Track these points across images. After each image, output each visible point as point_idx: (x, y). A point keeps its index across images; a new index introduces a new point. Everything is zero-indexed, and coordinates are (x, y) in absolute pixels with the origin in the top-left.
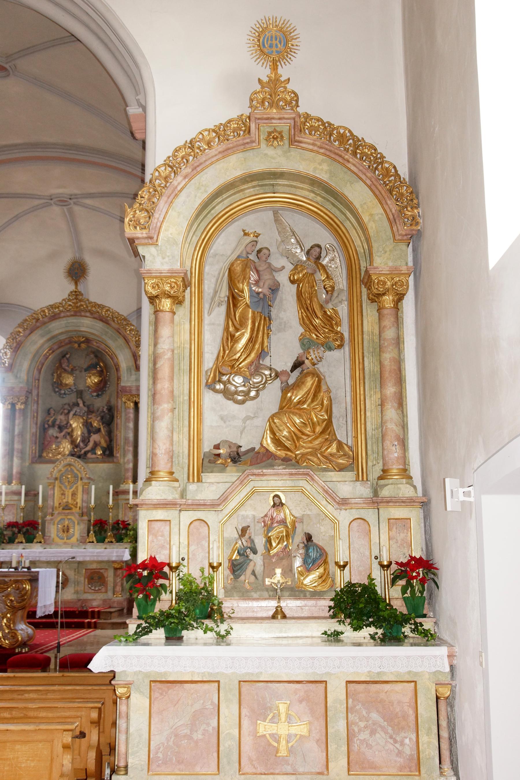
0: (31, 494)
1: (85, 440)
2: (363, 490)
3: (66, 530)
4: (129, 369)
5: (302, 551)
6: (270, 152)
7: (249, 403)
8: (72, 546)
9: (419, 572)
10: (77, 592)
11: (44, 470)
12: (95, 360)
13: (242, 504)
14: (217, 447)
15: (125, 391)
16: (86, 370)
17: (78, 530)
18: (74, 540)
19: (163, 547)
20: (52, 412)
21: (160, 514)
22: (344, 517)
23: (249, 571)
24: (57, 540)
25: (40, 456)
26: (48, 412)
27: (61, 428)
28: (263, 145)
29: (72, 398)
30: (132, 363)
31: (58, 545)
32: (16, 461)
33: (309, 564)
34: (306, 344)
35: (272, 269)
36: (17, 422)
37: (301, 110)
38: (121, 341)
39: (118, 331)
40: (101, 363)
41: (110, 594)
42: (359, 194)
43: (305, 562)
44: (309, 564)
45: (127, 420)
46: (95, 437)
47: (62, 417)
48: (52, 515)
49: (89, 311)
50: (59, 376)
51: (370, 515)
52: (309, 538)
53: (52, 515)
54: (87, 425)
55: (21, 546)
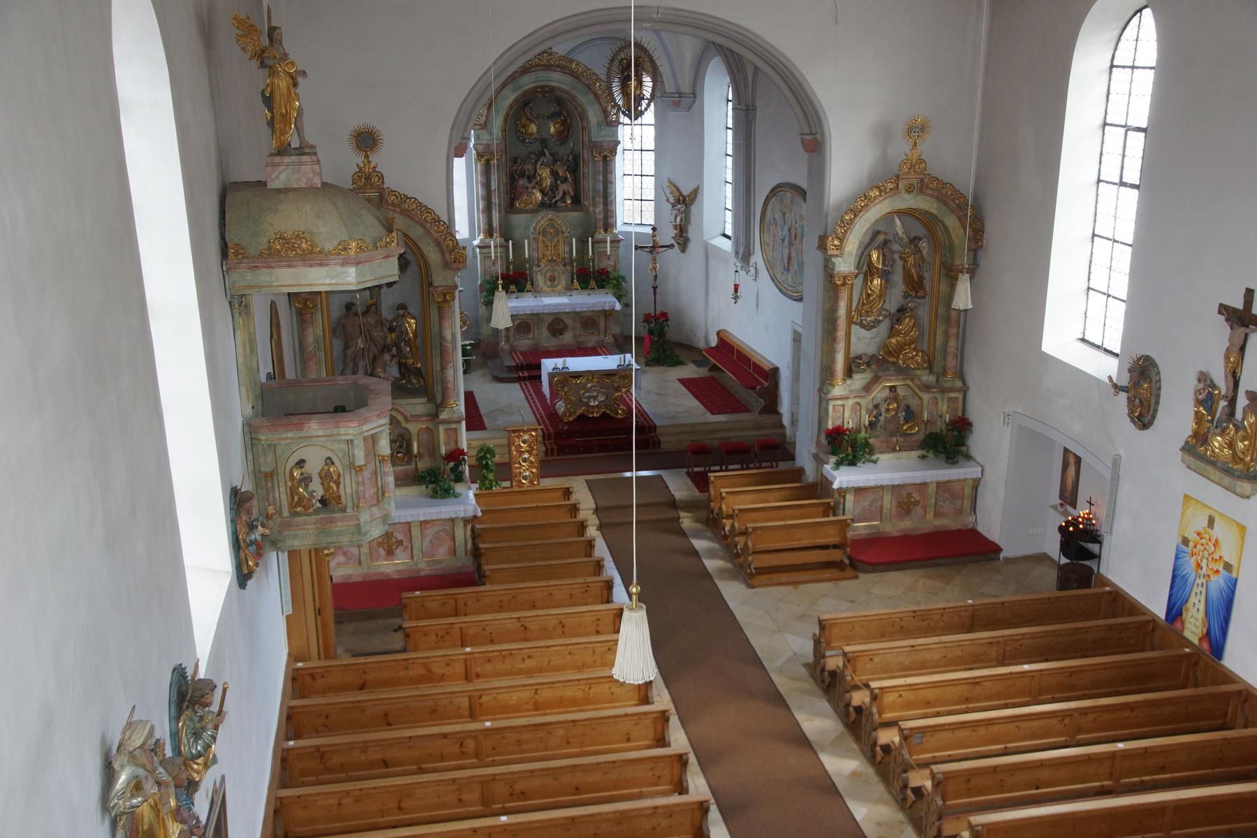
0: (518, 247)
1: (554, 188)
2: (932, 379)
3: (553, 279)
4: (599, 125)
6: (906, 196)
8: (560, 294)
9: (962, 426)
10: (574, 336)
11: (519, 220)
12: (557, 109)
14: (859, 357)
15: (595, 146)
16: (548, 118)
17: (563, 280)
18: (559, 288)
20: (519, 161)
21: (840, 402)
22: (926, 397)
24: (545, 288)
25: (512, 204)
26: (515, 160)
27: (530, 179)
29: (538, 147)
30: (601, 118)
31: (547, 294)
32: (496, 215)
33: (907, 420)
35: (893, 253)
36: (494, 177)
38: (591, 97)
39: (588, 86)
40: (563, 110)
41: (602, 336)
42: (951, 222)
44: (907, 420)
45: (596, 174)
46: (563, 187)
47: (529, 167)
48: (538, 266)
49: (558, 66)
50: (524, 126)
51: (939, 396)
52: (908, 407)
53: (538, 266)
54: (554, 174)
55: (514, 295)
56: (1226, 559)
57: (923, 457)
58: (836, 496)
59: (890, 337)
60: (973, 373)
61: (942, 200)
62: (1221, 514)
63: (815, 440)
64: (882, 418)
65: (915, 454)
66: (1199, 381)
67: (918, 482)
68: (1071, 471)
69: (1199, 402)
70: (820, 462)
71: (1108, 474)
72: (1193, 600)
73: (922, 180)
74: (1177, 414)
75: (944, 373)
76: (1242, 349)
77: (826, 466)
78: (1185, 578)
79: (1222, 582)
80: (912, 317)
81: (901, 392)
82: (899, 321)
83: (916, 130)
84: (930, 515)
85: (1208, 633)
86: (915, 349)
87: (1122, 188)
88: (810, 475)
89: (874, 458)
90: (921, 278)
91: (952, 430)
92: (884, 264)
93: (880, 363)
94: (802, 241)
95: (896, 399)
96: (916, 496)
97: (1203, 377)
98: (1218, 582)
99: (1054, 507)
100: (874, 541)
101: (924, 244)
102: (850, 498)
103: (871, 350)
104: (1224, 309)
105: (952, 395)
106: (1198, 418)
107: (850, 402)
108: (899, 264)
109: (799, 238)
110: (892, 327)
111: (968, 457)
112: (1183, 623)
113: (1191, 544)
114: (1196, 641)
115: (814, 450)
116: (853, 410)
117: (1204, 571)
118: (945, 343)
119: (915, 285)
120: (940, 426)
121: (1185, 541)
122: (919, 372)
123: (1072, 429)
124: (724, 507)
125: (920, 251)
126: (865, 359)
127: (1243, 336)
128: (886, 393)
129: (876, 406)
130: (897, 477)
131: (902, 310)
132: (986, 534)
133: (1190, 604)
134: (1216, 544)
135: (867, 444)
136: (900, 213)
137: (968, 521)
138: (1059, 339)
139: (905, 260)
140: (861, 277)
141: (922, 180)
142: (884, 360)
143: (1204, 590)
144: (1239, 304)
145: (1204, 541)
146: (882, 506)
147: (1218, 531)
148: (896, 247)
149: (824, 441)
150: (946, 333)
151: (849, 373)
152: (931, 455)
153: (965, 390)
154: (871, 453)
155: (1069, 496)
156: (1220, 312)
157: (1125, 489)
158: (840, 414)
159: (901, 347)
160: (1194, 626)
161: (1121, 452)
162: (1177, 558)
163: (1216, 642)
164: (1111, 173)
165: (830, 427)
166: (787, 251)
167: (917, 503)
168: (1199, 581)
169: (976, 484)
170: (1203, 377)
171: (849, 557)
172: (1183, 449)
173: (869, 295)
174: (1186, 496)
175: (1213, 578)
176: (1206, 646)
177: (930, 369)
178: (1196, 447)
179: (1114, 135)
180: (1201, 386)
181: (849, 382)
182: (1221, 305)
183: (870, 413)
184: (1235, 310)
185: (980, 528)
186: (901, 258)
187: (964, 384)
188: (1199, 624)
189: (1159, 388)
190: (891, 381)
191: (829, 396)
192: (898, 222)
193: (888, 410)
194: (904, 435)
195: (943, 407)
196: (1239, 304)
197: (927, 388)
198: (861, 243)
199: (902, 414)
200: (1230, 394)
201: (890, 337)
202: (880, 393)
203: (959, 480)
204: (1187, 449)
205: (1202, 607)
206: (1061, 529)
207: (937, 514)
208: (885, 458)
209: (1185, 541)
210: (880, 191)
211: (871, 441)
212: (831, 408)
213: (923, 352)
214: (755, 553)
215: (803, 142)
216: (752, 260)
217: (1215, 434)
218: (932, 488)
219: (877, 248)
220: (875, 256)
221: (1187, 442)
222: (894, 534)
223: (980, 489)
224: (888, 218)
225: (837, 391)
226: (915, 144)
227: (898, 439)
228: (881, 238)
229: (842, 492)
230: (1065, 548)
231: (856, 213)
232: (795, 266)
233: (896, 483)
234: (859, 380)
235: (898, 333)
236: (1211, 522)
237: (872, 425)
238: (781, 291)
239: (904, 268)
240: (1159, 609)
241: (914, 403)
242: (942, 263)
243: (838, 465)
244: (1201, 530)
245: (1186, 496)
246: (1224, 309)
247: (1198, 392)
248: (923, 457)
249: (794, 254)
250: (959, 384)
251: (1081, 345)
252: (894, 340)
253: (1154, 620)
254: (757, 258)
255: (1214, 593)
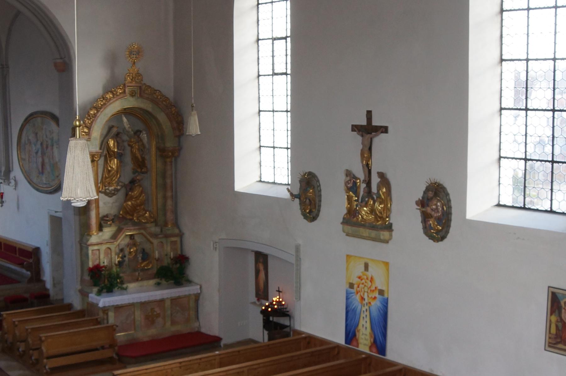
2: (158, 230)
5: (141, 255)
6: (131, 99)
7: (114, 197)
9: (182, 260)
13: (121, 241)
14: (107, 216)
19: (97, 259)
21: (96, 248)
22: (155, 242)
23: (125, 263)
28: (128, 95)
34: (134, 172)
35: (123, 141)
37: (143, 82)
42: (162, 117)
43: (142, 259)
44: (144, 259)
51: (164, 240)
52: (144, 250)
56: (380, 288)
57: (158, 284)
58: (101, 314)
59: (126, 201)
60: (186, 222)
61: (154, 102)
62: (372, 260)
63: (79, 279)
64: (126, 259)
65: (152, 282)
66: (347, 176)
67: (158, 298)
68: (262, 275)
69: (349, 189)
70: (84, 294)
71: (293, 260)
72: (362, 322)
73: (140, 87)
74: (334, 203)
75: (166, 224)
76: (370, 149)
77: (90, 295)
78: (354, 310)
79: (379, 304)
80: (140, 186)
81: (138, 239)
82: (131, 190)
83: (136, 53)
84: (168, 324)
85: (375, 341)
86: (144, 209)
87: (275, 77)
88: (78, 305)
89: (125, 286)
90: (144, 159)
91: (176, 263)
92: (118, 149)
93: (122, 219)
94: (52, 149)
95: (135, 245)
96: (157, 310)
97: (348, 173)
98: (376, 304)
99: (254, 303)
100: (133, 345)
101: (144, 136)
102: (111, 314)
103: (113, 211)
104: (356, 128)
105: (173, 239)
106: (349, 199)
107: (103, 248)
108: (128, 149)
109: (50, 148)
110: (127, 195)
111: (189, 282)
112: (357, 340)
113: (355, 286)
114: (367, 350)
115: (79, 287)
116: (106, 254)
117: (366, 301)
118: (165, 205)
119: (140, 165)
120: (166, 262)
121: (351, 286)
122: (148, 225)
123: (262, 238)
124: (18, 333)
125: (141, 140)
126: (111, 218)
127: (370, 140)
128: (127, 240)
129: (122, 250)
130: (144, 297)
131: (133, 182)
132: (209, 333)
133: (360, 327)
134: (372, 280)
135: (118, 276)
136: (126, 112)
137: (194, 326)
138: (245, 180)
139: (131, 147)
140: (103, 158)
141: (140, 87)
142: (124, 218)
143: (368, 313)
144: (364, 122)
145: (363, 281)
146: (134, 319)
147: (372, 271)
148: (125, 138)
149: (87, 278)
150: (165, 198)
151: (100, 228)
152: (164, 282)
153: (181, 235)
154: (122, 283)
155: (262, 293)
156: (353, 130)
157: (306, 265)
158: (97, 257)
159: (134, 209)
160: (364, 344)
161: (300, 242)
162: (347, 299)
163: (380, 345)
164: (266, 69)
165: (91, 265)
166: (40, 160)
167: (158, 315)
168: (364, 309)
169: (197, 297)
170: (348, 173)
171: (117, 354)
172: (343, 223)
173: (109, 171)
174: (347, 256)
175: (373, 303)
176: (374, 349)
177: (156, 222)
178: (351, 219)
179: (265, 46)
180: (348, 178)
181: (101, 234)
182: (352, 126)
183: (118, 254)
184: (361, 126)
185: (203, 330)
186: (129, 145)
187: (180, 231)
188: (368, 337)
189: (320, 191)
190: (130, 230)
191: (89, 243)
192: (125, 119)
193: (130, 253)
194: (143, 270)
195: (168, 248)
196: (364, 122)
197: (155, 236)
198: (101, 135)
199: (140, 257)
200: (367, 179)
201: (126, 201)
202: (123, 241)
203: (186, 296)
204: (346, 221)
205: (368, 325)
206: (263, 312)
207: (173, 323)
208: (132, 286)
209: (351, 286)
210: (113, 94)
211: (121, 275)
212: (90, 252)
213: (150, 212)
214: (48, 358)
215: (56, 65)
216: (12, 175)
217: (363, 207)
218: (168, 303)
219: (112, 138)
220: (111, 143)
221: (344, 218)
222: (146, 339)
223: (200, 302)
224: (117, 116)
225: (94, 239)
226: (134, 63)
227: (140, 275)
228: (115, 130)
229: (105, 310)
230: (267, 325)
231: (98, 109)
232: (48, 168)
233: (143, 300)
234: (108, 232)
235: (131, 199)
236: (366, 267)
237: (120, 264)
238: (37, 190)
239: (132, 152)
240: (340, 339)
241: (147, 247)
242: (158, 148)
243: (99, 293)
244: (361, 274)
245: (347, 256)
246: (356, 128)
247: (346, 183)
248: (158, 284)
249: (46, 160)
250: (177, 231)
251: (260, 184)
252: (130, 203)
253: (337, 347)
254: (17, 172)
255: (375, 313)
